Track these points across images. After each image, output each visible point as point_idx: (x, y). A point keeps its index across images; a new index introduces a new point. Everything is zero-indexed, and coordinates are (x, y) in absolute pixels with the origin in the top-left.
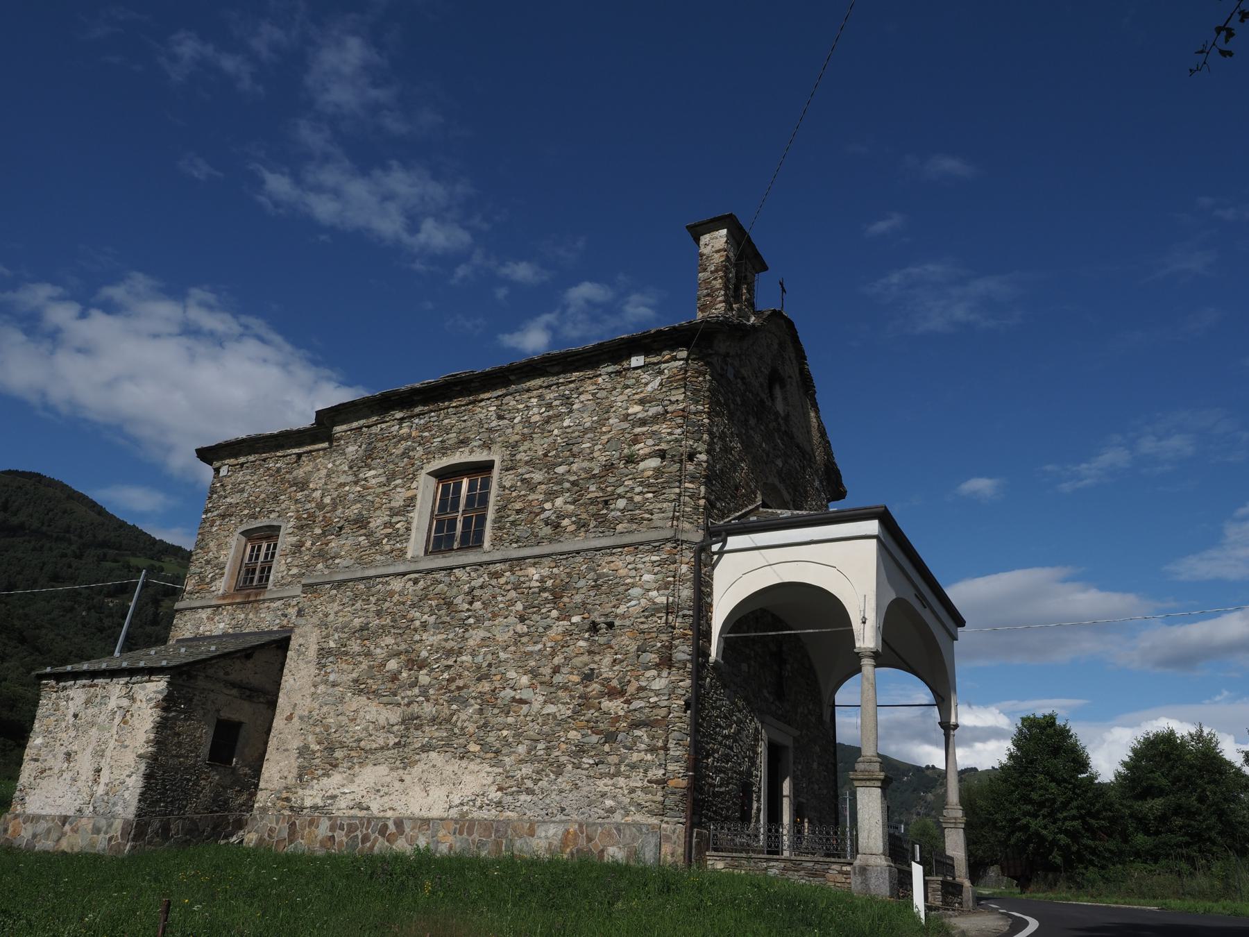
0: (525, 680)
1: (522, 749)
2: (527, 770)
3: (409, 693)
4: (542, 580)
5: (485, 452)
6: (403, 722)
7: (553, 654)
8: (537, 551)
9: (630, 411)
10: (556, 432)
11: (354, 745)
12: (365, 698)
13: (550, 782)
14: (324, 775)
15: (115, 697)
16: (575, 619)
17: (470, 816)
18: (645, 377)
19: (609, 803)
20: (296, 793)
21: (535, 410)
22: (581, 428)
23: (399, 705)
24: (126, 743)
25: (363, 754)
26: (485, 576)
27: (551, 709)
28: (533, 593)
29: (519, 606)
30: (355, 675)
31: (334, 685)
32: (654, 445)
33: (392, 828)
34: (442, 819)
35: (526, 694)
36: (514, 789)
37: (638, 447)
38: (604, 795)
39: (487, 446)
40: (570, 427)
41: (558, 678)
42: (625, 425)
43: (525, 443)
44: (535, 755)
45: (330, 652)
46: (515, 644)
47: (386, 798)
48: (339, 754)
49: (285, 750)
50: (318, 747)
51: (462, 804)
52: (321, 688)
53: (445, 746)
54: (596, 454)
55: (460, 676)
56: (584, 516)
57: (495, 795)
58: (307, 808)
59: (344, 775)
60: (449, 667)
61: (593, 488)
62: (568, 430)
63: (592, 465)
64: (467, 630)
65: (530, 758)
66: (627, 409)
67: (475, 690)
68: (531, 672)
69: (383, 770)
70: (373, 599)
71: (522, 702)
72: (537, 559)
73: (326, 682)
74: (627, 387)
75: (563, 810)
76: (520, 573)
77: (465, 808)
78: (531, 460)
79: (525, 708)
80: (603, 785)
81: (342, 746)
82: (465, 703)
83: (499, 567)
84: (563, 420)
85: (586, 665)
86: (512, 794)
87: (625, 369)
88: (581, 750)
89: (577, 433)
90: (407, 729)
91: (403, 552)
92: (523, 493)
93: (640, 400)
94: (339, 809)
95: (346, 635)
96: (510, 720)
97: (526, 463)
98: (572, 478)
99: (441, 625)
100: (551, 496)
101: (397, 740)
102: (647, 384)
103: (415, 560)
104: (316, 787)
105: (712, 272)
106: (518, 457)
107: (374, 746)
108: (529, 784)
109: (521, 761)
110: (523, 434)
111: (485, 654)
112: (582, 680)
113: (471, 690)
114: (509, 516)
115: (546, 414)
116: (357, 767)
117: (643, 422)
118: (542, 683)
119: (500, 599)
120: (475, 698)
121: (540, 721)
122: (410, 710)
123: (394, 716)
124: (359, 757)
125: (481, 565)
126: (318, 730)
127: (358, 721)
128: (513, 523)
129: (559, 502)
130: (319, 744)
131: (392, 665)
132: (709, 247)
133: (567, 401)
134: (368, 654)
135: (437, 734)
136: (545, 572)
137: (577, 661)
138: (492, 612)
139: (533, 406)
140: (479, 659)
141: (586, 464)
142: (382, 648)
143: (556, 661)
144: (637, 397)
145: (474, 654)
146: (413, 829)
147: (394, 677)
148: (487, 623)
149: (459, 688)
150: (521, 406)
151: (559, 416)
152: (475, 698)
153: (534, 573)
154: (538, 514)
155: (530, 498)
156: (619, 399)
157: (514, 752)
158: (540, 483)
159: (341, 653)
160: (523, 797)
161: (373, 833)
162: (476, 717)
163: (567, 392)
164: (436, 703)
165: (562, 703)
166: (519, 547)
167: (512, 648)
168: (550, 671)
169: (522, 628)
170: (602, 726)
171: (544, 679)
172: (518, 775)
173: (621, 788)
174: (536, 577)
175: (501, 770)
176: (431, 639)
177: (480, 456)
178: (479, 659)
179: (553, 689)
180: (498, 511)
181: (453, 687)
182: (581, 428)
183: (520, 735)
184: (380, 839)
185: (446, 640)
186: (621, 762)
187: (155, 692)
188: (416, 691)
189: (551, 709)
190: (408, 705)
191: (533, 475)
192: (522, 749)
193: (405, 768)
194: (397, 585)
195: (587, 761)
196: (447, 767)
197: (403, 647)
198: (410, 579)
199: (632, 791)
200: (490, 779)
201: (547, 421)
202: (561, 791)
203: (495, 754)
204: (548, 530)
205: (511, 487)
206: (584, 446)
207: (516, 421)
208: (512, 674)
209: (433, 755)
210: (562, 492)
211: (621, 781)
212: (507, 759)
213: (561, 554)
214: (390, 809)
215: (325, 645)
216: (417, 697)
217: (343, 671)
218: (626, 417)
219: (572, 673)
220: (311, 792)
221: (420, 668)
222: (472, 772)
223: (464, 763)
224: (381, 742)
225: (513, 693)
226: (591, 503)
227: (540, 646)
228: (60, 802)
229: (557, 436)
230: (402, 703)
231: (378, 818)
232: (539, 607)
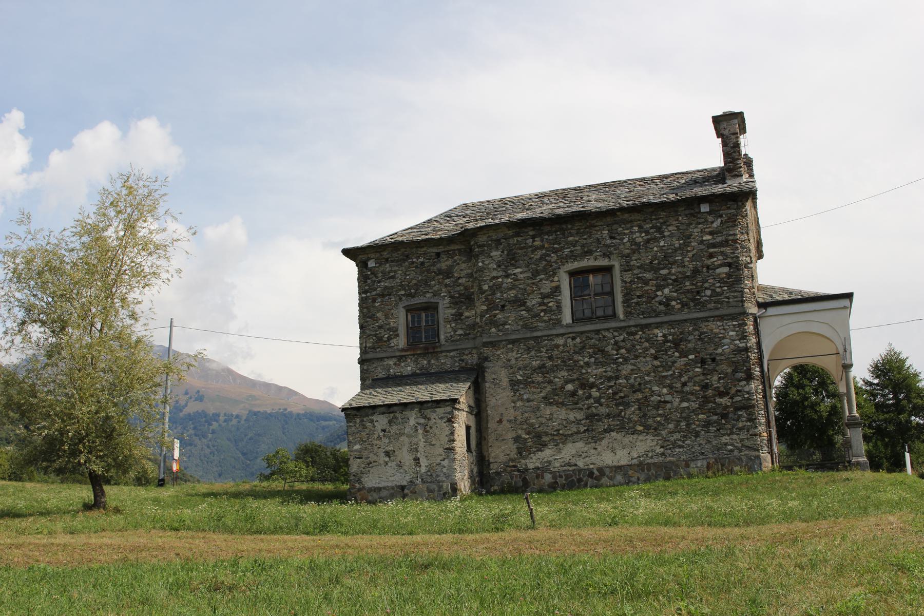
0: (665, 391)
1: (671, 426)
2: (676, 436)
3: (587, 402)
4: (664, 336)
5: (607, 260)
6: (587, 418)
7: (681, 376)
8: (658, 320)
9: (704, 238)
10: (655, 249)
11: (555, 433)
12: (555, 407)
13: (693, 441)
14: (538, 451)
15: (413, 418)
16: (691, 357)
17: (646, 462)
18: (710, 218)
19: (730, 447)
20: (520, 462)
21: (638, 235)
22: (673, 247)
23: (582, 409)
24: (433, 443)
25: (561, 438)
26: (625, 334)
27: (685, 404)
28: (660, 344)
29: (653, 351)
30: (542, 395)
31: (529, 400)
32: (724, 259)
33: (596, 473)
34: (628, 465)
35: (668, 398)
36: (671, 446)
37: (712, 260)
38: (726, 444)
39: (607, 255)
40: (664, 246)
41: (687, 389)
42: (702, 247)
43: (635, 255)
44: (681, 429)
45: (519, 382)
46: (654, 372)
47: (587, 459)
48: (545, 439)
49: (503, 440)
50: (528, 436)
51: (639, 457)
52: (519, 404)
53: (621, 428)
54: (687, 263)
55: (621, 391)
56: (685, 300)
57: (659, 450)
58: (530, 469)
59: (553, 450)
60: (611, 387)
61: (687, 283)
62: (664, 248)
63: (685, 270)
64: (619, 366)
65: (677, 430)
66: (702, 237)
67: (633, 398)
68: (668, 386)
69: (580, 445)
70: (544, 350)
71: (666, 402)
72: (659, 325)
73: (522, 400)
74: (700, 223)
75: (703, 454)
76: (649, 332)
77: (642, 459)
78: (641, 265)
79: (669, 406)
80: (725, 439)
81: (547, 434)
82: (627, 405)
83: (633, 329)
84: (659, 242)
85: (703, 381)
86: (670, 449)
87: (696, 213)
88: (707, 424)
89: (670, 251)
90: (591, 422)
91: (559, 322)
92: (640, 285)
93: (709, 232)
94: (554, 468)
95: (529, 372)
96: (660, 412)
97: (638, 267)
98: (673, 277)
99: (598, 364)
100: (660, 288)
101: (586, 428)
102: (712, 223)
103: (568, 326)
104: (534, 458)
105: (731, 147)
106: (632, 263)
107: (570, 432)
108: (680, 443)
109: (673, 432)
110: (632, 249)
111: (635, 378)
112: (702, 388)
113: (630, 398)
114: (633, 299)
115: (645, 238)
116: (561, 445)
117: (714, 246)
118: (677, 392)
119: (638, 347)
120: (634, 402)
121: (679, 411)
122: (590, 411)
123: (580, 415)
124: (560, 439)
125: (620, 328)
126: (525, 427)
127: (554, 420)
128: (637, 303)
129: (666, 291)
130: (528, 434)
131: (570, 387)
132: (727, 130)
133: (659, 230)
134: (550, 382)
135: (613, 423)
136: (666, 331)
137: (697, 379)
138: (634, 355)
139: (636, 232)
140: (632, 381)
141: (680, 269)
142: (560, 378)
143: (683, 379)
144: (707, 230)
145: (627, 378)
146: (610, 472)
147: (573, 394)
148: (632, 361)
149: (621, 397)
150: (626, 232)
151: (656, 240)
152: (634, 402)
153: (659, 333)
154: (654, 298)
155: (646, 288)
156: (696, 232)
157: (666, 428)
158: (651, 280)
159: (527, 382)
160: (677, 450)
161: (584, 477)
162: (637, 412)
163: (658, 224)
164: (608, 406)
165: (692, 401)
166: (644, 317)
167: (653, 374)
168: (680, 385)
169: (657, 363)
170: (718, 411)
171: (677, 390)
172: (672, 439)
173: (736, 440)
174: (660, 334)
175: (660, 438)
176: (595, 371)
177: (604, 262)
178: (632, 381)
179: (684, 395)
180: (624, 296)
181: (617, 397)
182: (673, 247)
183: (668, 419)
184: (590, 480)
185: (605, 372)
186: (733, 427)
187: (444, 413)
188: (592, 401)
189: (685, 404)
190: (588, 408)
191: (645, 275)
192: (671, 426)
193: (596, 442)
194: (560, 341)
195: (712, 429)
196: (626, 439)
197: (575, 377)
198: (569, 337)
199: (742, 440)
200: (655, 443)
201: (648, 241)
202: (700, 445)
203: (655, 430)
204: (662, 308)
205: (631, 281)
206: (677, 258)
207: (625, 240)
208: (656, 388)
209: (612, 434)
210: (668, 285)
211: (735, 437)
212: (663, 432)
213: (675, 321)
214: (591, 464)
215: (514, 378)
216: (593, 404)
217: (534, 393)
218: (702, 242)
219: (694, 386)
220: (531, 461)
221: (592, 388)
222: (642, 441)
223: (635, 436)
224: (575, 430)
225: (659, 398)
226: (688, 292)
227: (670, 372)
228: (392, 479)
229: (656, 251)
230: (584, 408)
231: (585, 469)
232: (666, 351)
